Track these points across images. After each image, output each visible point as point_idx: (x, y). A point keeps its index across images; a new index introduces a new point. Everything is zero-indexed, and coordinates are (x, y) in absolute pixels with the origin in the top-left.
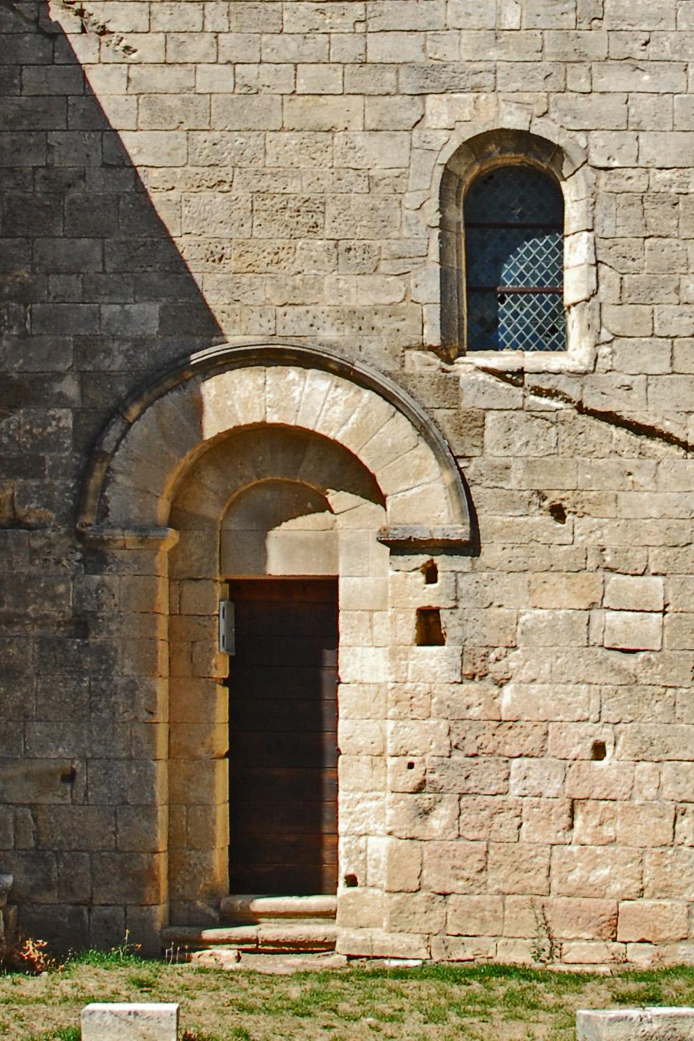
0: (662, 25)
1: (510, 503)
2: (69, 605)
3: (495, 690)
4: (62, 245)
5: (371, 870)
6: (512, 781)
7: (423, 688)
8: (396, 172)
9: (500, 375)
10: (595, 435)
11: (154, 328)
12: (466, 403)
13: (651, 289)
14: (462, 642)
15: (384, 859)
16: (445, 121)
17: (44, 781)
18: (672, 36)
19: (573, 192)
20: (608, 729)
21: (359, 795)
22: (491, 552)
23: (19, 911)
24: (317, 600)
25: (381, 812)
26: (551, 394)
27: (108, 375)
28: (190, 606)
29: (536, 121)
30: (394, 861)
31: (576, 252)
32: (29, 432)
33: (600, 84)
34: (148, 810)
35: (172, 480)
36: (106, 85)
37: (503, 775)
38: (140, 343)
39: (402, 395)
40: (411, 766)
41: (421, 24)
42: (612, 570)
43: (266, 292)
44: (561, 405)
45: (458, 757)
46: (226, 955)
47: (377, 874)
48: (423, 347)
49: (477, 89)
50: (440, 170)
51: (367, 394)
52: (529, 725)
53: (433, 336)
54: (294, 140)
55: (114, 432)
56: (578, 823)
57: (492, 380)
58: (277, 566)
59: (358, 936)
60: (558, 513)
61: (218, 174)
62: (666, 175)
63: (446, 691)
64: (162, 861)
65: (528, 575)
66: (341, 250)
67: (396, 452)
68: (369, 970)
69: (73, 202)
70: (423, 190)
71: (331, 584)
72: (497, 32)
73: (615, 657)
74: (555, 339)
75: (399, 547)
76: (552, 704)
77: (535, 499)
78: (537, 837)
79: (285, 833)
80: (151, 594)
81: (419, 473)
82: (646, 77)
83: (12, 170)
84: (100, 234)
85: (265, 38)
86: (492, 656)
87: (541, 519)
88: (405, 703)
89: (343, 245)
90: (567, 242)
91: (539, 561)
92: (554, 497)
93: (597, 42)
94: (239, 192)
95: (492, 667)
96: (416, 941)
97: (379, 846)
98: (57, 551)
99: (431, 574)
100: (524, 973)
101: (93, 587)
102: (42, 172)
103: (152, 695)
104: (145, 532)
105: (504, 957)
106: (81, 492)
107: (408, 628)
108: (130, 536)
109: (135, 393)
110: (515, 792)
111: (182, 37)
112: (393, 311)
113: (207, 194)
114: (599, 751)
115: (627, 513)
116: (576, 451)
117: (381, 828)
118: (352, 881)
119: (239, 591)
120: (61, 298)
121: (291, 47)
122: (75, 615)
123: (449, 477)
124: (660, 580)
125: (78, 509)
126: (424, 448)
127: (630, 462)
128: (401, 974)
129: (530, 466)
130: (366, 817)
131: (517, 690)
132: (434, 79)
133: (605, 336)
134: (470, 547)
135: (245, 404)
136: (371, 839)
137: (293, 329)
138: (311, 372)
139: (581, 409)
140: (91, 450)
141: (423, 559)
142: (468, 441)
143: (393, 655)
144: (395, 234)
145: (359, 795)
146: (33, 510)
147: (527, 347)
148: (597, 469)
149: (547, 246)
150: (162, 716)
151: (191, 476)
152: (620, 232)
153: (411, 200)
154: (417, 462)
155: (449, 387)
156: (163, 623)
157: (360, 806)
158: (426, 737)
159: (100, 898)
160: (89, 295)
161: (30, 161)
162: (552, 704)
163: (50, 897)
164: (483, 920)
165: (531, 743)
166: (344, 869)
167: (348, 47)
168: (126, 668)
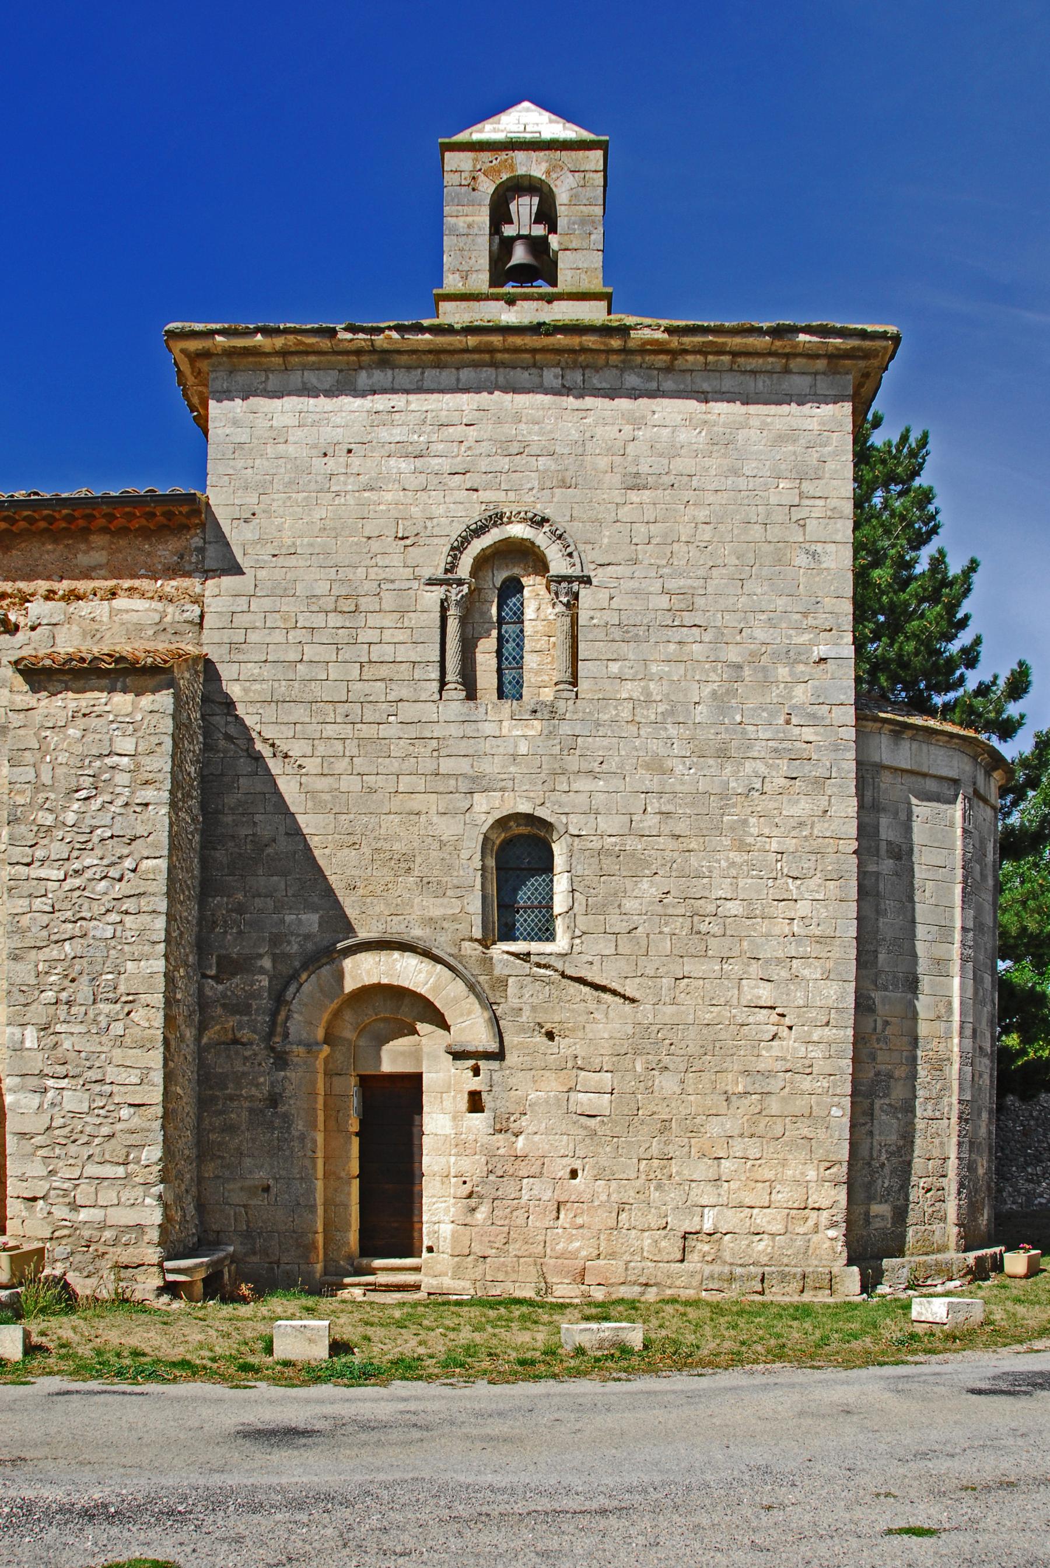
0: (610, 753)
1: (522, 1030)
2: (266, 1089)
3: (514, 1139)
4: (262, 880)
5: (441, 1243)
6: (523, 1192)
7: (472, 1137)
8: (456, 838)
9: (517, 955)
10: (572, 991)
11: (315, 928)
12: (497, 972)
13: (604, 905)
14: (495, 1110)
15: (449, 1237)
16: (485, 808)
17: (252, 1191)
18: (617, 759)
19: (559, 850)
20: (579, 1162)
21: (434, 1200)
22: (511, 1058)
23: (237, 1267)
24: (411, 1085)
25: (447, 1210)
26: (546, 966)
27: (288, 956)
28: (337, 1090)
29: (538, 808)
30: (455, 1238)
31: (561, 884)
32: (243, 989)
33: (575, 786)
34: (312, 1208)
35: (326, 1017)
36: (288, 787)
37: (518, 1188)
38: (307, 937)
39: (460, 967)
40: (465, 1182)
41: (471, 752)
42: (581, 1069)
43: (380, 907)
44: (552, 973)
45: (492, 1177)
46: (358, 1292)
47: (445, 1245)
48: (471, 940)
49: (503, 790)
50: (482, 836)
51: (439, 967)
52: (534, 1159)
53: (478, 933)
54: (397, 819)
55: (292, 989)
56: (562, 1216)
57: (512, 958)
58: (387, 1066)
59: (434, 1282)
60: (550, 1036)
62: (613, 839)
63: (484, 1139)
64: (320, 1238)
65: (533, 1072)
66: (424, 883)
67: (456, 1000)
68: (440, 1301)
69: (268, 855)
70: (473, 847)
71: (418, 1077)
72: (514, 756)
73: (583, 1119)
74: (551, 937)
75: (458, 1055)
76: (547, 1147)
77: (537, 1028)
78: (538, 1224)
79: (391, 1220)
80: (314, 1083)
81: (469, 1013)
82: (601, 783)
83: (233, 836)
84: (284, 874)
85: (380, 760)
86: (512, 1119)
87: (540, 1039)
88: (461, 1146)
89: (425, 880)
90: (555, 878)
91: (538, 1064)
92: (548, 1026)
93: (573, 762)
94: (366, 850)
95: (512, 1125)
96: (468, 1284)
97: (446, 1229)
98: (259, 1058)
99: (476, 1071)
100: (530, 1303)
101: (280, 1079)
102: (250, 838)
103: (314, 1142)
104: (310, 1046)
105: (519, 1294)
106: (273, 1023)
107: (463, 1103)
108: (301, 1049)
109: (305, 966)
110: (525, 1198)
111: (332, 759)
112: (454, 919)
113: (346, 851)
114: (574, 1174)
115: (590, 1036)
116: (560, 1000)
117: (447, 1219)
118: (430, 1250)
119: (365, 1081)
120: (261, 911)
121: (395, 766)
122: (270, 1095)
123: (487, 1015)
124: (609, 1075)
125: (271, 1034)
126: (472, 998)
127: (592, 1006)
128: (459, 1303)
129: (534, 1009)
130: (439, 1212)
131: (527, 1139)
132: (478, 784)
133: (578, 933)
134: (499, 1056)
135: (368, 972)
136: (442, 1225)
137: (396, 929)
138: (407, 954)
139: (563, 975)
140: (279, 1000)
141: (471, 1063)
142: (498, 994)
143: (454, 1118)
144: (455, 874)
145: (434, 1200)
146: (245, 1034)
147: (532, 940)
148: (573, 1011)
149: (544, 881)
150: (320, 1154)
151: (337, 1014)
152: (586, 873)
153: (465, 854)
154: (468, 1006)
155: (487, 962)
156: (321, 1100)
157: (435, 1206)
158: (473, 1166)
159: (284, 1260)
160: (277, 910)
161: (243, 831)
162: (547, 1147)
163: (255, 1259)
164: (506, 1272)
165: (535, 1170)
166: (426, 1242)
167: (429, 766)
168: (300, 1125)
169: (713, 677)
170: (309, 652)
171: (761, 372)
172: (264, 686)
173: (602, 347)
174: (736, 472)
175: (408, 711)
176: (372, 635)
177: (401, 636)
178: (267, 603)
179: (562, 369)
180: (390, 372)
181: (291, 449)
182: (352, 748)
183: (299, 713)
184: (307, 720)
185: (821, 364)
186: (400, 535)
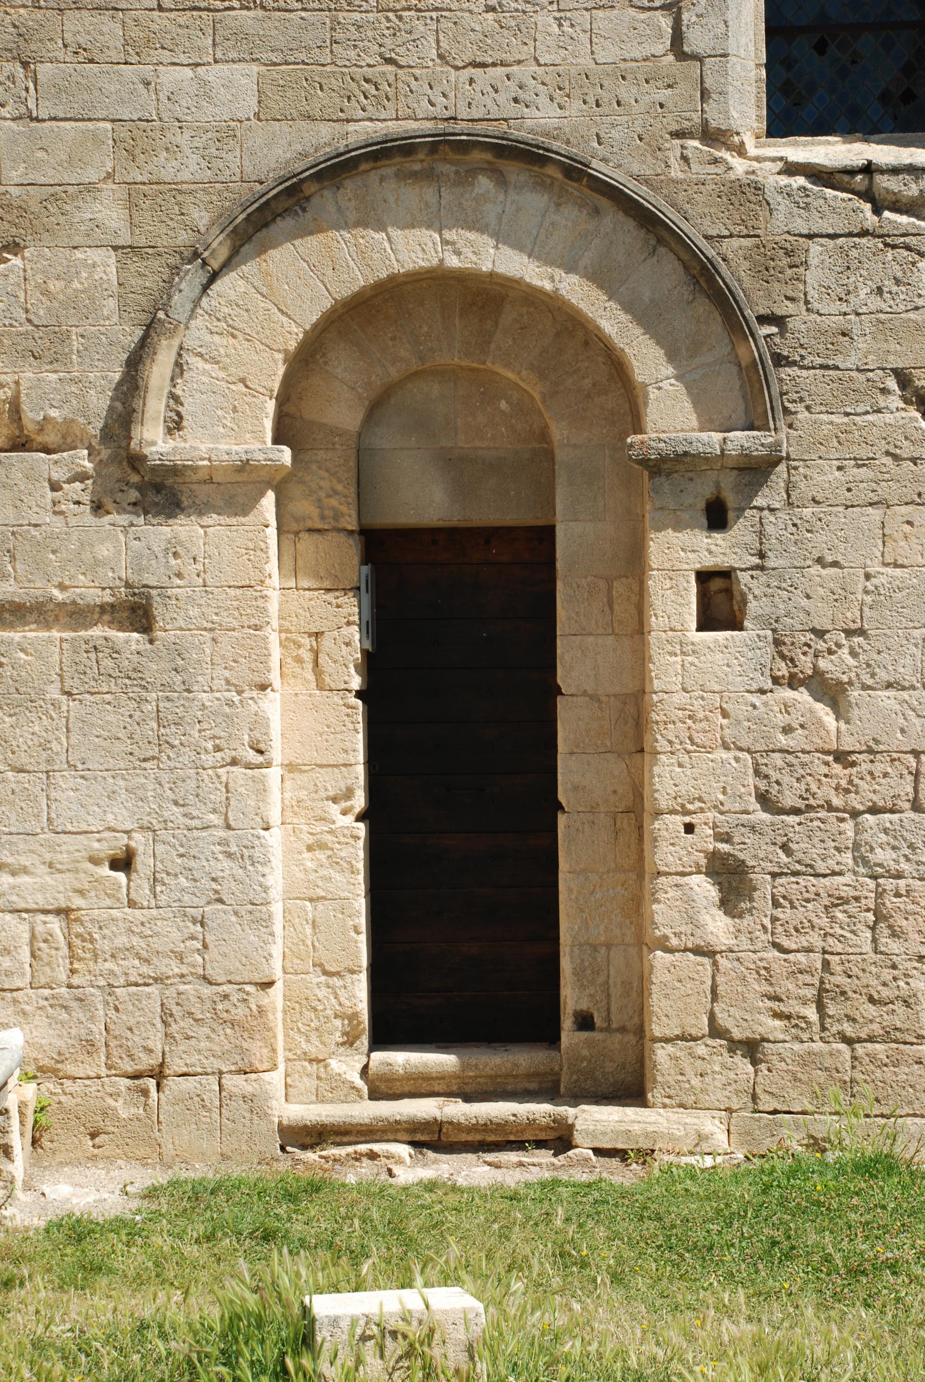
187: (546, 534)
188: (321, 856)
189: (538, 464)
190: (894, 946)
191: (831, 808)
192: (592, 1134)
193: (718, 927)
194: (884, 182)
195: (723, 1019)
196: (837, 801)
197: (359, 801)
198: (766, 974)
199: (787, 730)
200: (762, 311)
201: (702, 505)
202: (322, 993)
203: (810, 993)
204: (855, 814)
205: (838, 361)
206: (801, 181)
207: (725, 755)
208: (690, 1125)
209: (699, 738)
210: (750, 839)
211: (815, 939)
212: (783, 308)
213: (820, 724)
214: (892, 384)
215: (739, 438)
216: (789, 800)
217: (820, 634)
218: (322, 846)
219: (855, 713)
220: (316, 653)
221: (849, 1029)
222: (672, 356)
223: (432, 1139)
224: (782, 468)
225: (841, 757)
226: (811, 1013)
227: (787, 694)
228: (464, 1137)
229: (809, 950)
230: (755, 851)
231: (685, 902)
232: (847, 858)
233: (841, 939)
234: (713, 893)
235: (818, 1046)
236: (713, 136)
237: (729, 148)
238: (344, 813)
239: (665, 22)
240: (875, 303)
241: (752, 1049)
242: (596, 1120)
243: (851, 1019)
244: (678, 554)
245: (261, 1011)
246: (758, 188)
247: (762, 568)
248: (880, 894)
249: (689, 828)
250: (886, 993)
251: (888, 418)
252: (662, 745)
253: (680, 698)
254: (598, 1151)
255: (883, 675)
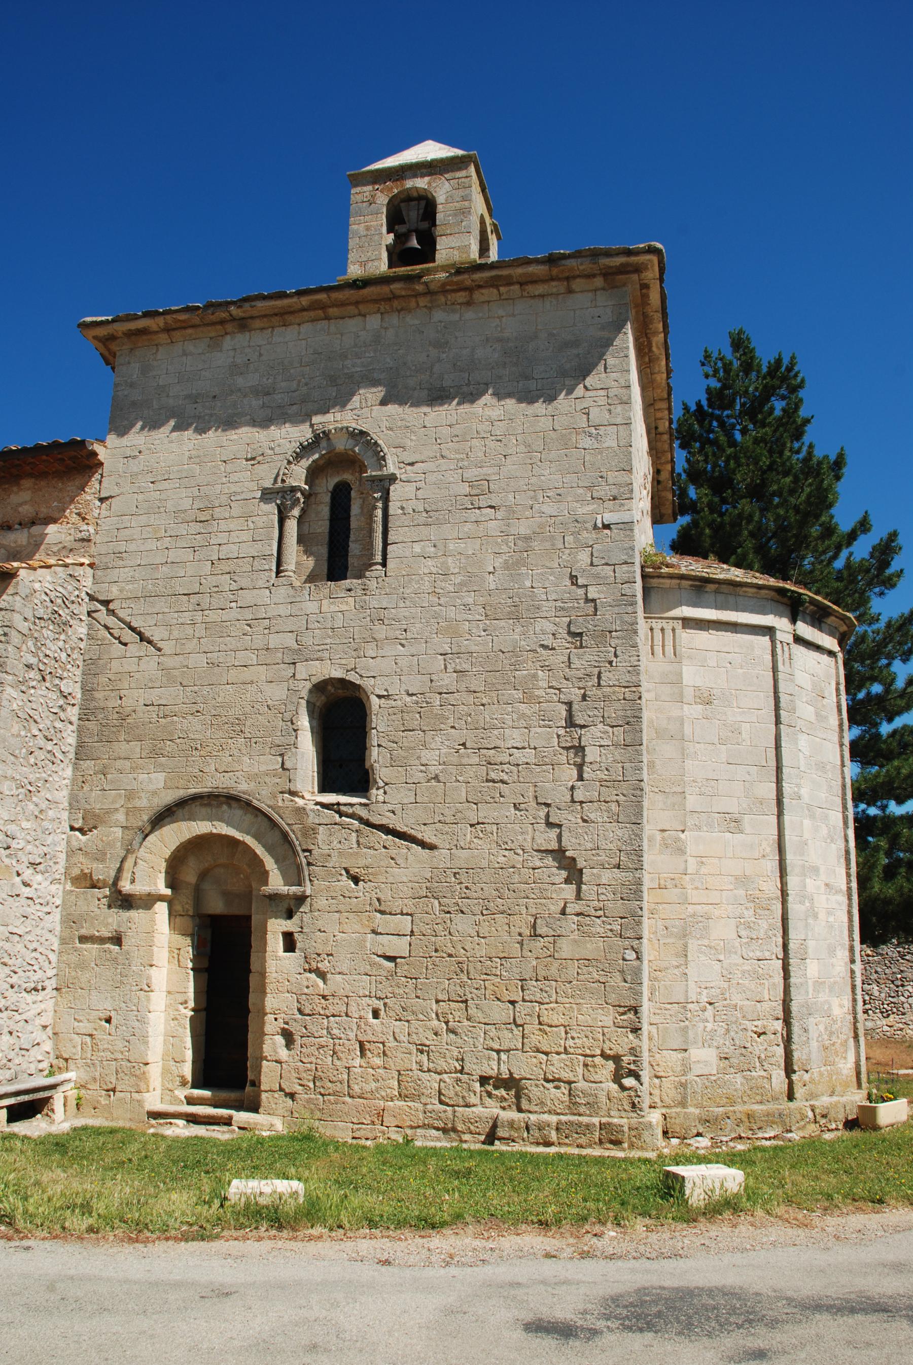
4: (124, 746)
26: (352, 816)
27: (140, 809)
60: (356, 880)
61: (196, 707)
89: (254, 740)
111: (183, 641)
121: (232, 643)
139: (368, 823)
161: (111, 704)
169: (505, 548)
170: (173, 556)
171: (548, 295)
172: (136, 586)
173: (410, 293)
174: (527, 378)
175: (247, 597)
176: (222, 538)
177: (246, 536)
178: (143, 519)
179: (382, 314)
180: (247, 334)
181: (171, 401)
182: (200, 631)
183: (161, 605)
184: (167, 610)
185: (599, 282)
186: (249, 456)
187: (248, 918)
188: (176, 1022)
189: (247, 896)
190: (338, 1063)
191: (320, 1015)
192: (238, 1122)
193: (283, 1053)
194: (343, 808)
195: (283, 1086)
196: (322, 1012)
197: (191, 1004)
198: (297, 1070)
199: (308, 987)
200: (304, 848)
201: (284, 910)
202: (174, 1068)
203: (311, 1078)
204: (328, 1017)
205: (327, 864)
206: (318, 807)
207: (288, 995)
208: (270, 1121)
209: (280, 989)
210: (294, 1024)
211: (313, 1059)
212: (311, 847)
213: (318, 986)
214: (343, 872)
215: (294, 889)
216: (307, 1011)
217: (319, 955)
218: (177, 1019)
219: (328, 982)
220: (179, 955)
221: (322, 1091)
222: (276, 862)
223: (193, 1119)
224: (309, 899)
225: (324, 997)
226: (311, 1085)
227: (308, 975)
228: (203, 1120)
229: (311, 1063)
230: (294, 1028)
231: (273, 1045)
232: (325, 1032)
233: (321, 1059)
234: (283, 1042)
235: (313, 1096)
236: (293, 793)
237: (299, 797)
238: (185, 1008)
239: (280, 759)
240: (339, 846)
241: (292, 1096)
242: (241, 1117)
243: (323, 1088)
244: (276, 927)
245: (144, 1073)
246: (304, 809)
247: (301, 932)
248: (334, 1045)
249: (276, 1019)
250: (334, 1079)
251: (342, 883)
252: (268, 990)
253: (274, 975)
254: (239, 1128)
255: (338, 970)
